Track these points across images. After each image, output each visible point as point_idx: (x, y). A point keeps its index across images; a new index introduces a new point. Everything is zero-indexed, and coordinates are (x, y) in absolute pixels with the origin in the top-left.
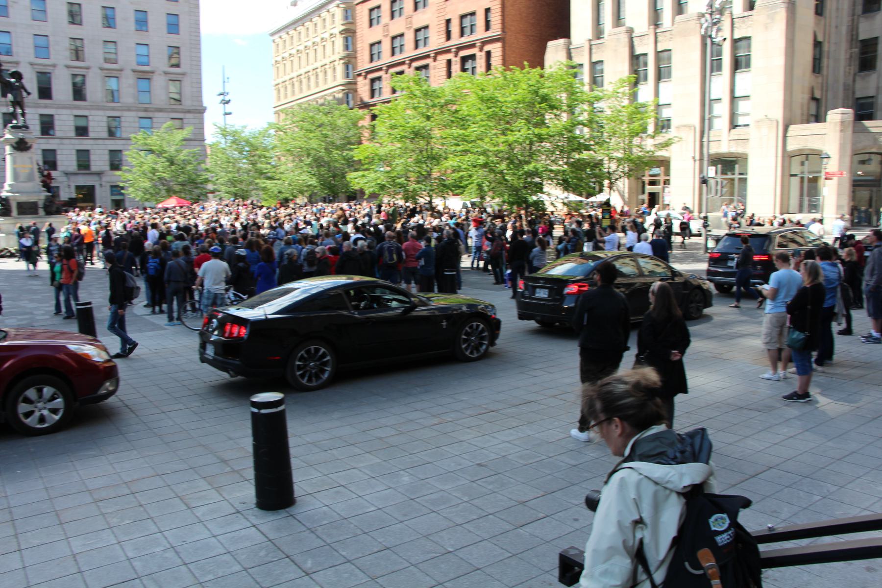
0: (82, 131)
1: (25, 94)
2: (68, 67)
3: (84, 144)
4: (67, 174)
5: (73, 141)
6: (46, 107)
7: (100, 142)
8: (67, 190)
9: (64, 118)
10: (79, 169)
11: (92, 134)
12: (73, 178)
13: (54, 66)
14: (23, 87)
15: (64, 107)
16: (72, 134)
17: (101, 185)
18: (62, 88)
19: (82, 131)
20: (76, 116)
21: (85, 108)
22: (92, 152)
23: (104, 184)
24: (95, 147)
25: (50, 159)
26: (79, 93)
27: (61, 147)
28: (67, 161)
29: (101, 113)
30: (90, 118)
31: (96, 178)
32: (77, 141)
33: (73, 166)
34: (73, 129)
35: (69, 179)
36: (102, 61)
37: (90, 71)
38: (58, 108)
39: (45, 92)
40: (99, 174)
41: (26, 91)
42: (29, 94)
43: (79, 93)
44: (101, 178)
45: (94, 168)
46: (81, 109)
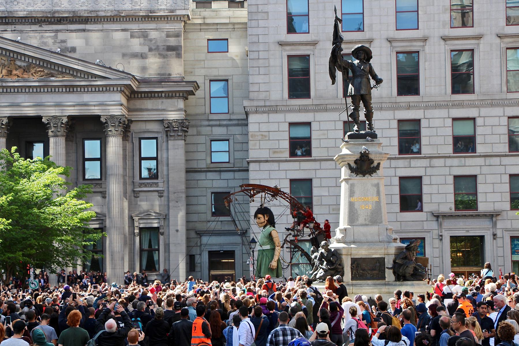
0: (465, 144)
1: (373, 82)
2: (445, 39)
3: (468, 165)
4: (438, 217)
5: (449, 162)
6: (409, 107)
7: (496, 161)
8: (437, 242)
9: (437, 123)
10: (457, 208)
11: (480, 149)
12: (447, 223)
13: (425, 40)
14: (371, 72)
15: (438, 106)
16: (450, 149)
17: (494, 235)
18: (435, 77)
19: (465, 144)
20: (454, 119)
21: (471, 105)
22: (480, 179)
23: (499, 233)
24: (485, 170)
25: (412, 191)
26: (462, 80)
27: (429, 171)
28: (439, 194)
29: (498, 111)
30: (479, 121)
31: (486, 223)
32: (455, 162)
33: (448, 204)
34: (450, 140)
35: (440, 225)
36: (503, 22)
37: (482, 41)
38: (427, 108)
39: (408, 84)
40: (492, 216)
41: (375, 77)
42: (379, 81)
43: (462, 80)
44: (495, 225)
45: (482, 207)
46: (465, 106)
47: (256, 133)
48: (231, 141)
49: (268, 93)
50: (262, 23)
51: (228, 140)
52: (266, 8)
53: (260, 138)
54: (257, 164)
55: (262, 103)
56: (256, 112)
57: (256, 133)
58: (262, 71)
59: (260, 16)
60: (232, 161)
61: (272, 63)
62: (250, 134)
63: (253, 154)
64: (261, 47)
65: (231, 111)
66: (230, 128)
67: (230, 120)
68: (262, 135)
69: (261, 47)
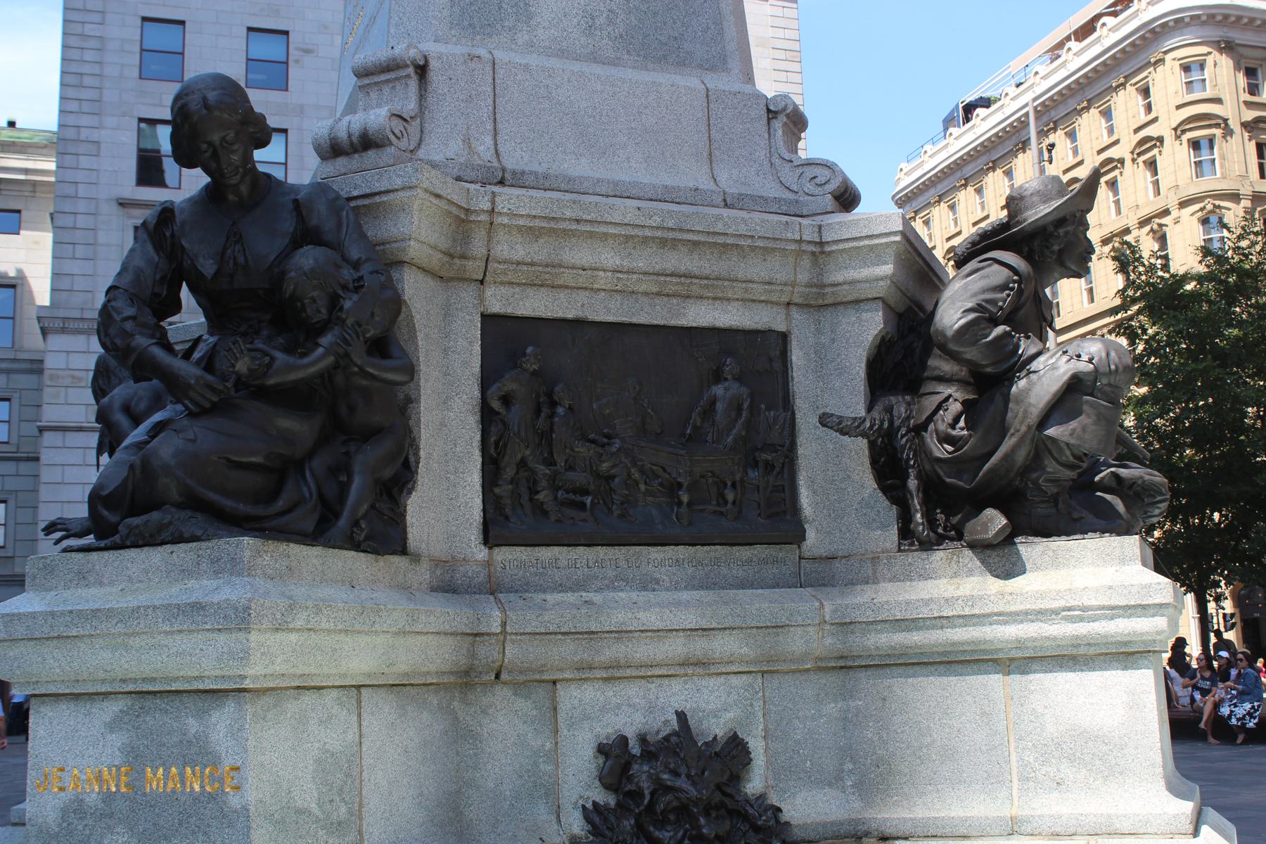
47: (60, 373)
48: (15, 401)
49: (90, 295)
50: (85, 162)
51: (8, 400)
52: (95, 135)
53: (68, 382)
54: (59, 434)
55: (77, 314)
56: (63, 330)
57: (60, 373)
58: (80, 251)
59: (82, 148)
60: (14, 440)
61: (102, 237)
62: (47, 373)
63: (51, 414)
64: (82, 207)
65: (17, 346)
66: (14, 377)
67: (15, 360)
68: (73, 377)
69: (82, 207)
